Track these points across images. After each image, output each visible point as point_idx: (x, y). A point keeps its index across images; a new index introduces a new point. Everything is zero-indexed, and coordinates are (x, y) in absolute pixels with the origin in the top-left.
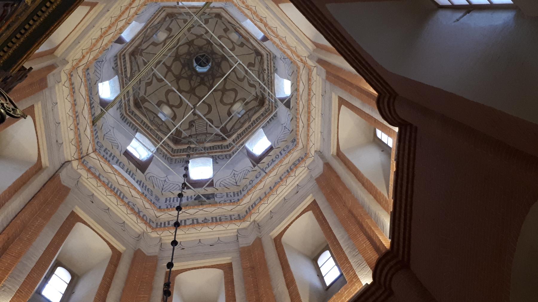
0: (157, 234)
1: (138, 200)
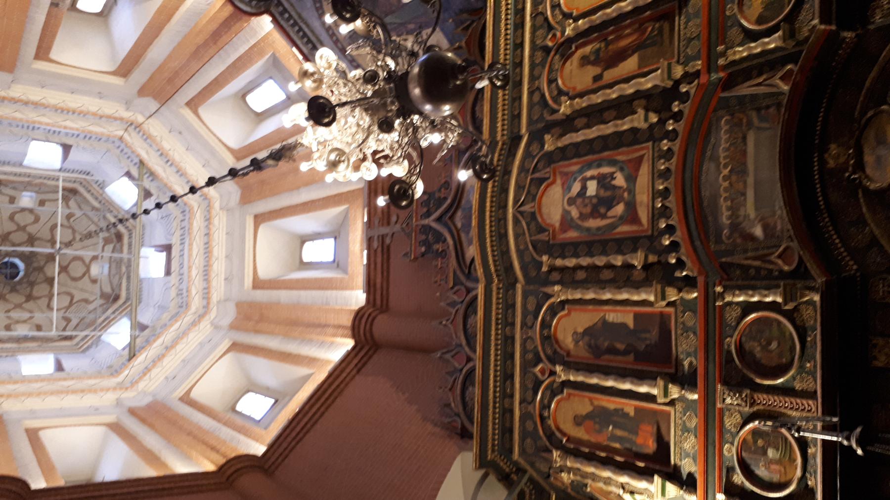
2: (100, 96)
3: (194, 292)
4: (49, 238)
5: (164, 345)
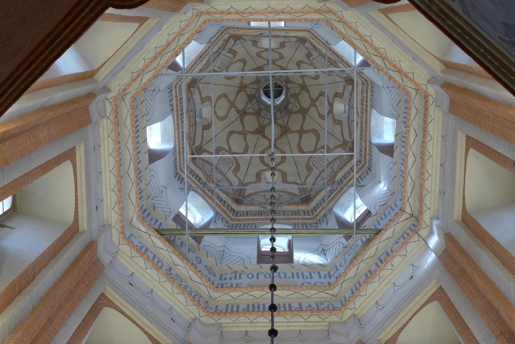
0: (427, 88)
1: (416, 127)
2: (442, 193)
3: (235, 294)
4: (306, 128)
5: (172, 266)
